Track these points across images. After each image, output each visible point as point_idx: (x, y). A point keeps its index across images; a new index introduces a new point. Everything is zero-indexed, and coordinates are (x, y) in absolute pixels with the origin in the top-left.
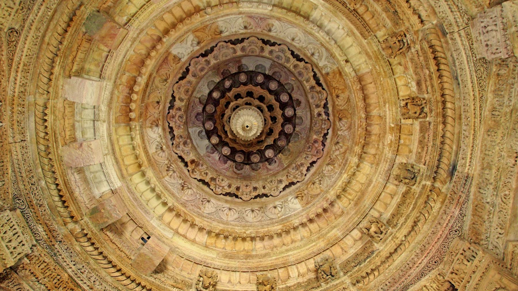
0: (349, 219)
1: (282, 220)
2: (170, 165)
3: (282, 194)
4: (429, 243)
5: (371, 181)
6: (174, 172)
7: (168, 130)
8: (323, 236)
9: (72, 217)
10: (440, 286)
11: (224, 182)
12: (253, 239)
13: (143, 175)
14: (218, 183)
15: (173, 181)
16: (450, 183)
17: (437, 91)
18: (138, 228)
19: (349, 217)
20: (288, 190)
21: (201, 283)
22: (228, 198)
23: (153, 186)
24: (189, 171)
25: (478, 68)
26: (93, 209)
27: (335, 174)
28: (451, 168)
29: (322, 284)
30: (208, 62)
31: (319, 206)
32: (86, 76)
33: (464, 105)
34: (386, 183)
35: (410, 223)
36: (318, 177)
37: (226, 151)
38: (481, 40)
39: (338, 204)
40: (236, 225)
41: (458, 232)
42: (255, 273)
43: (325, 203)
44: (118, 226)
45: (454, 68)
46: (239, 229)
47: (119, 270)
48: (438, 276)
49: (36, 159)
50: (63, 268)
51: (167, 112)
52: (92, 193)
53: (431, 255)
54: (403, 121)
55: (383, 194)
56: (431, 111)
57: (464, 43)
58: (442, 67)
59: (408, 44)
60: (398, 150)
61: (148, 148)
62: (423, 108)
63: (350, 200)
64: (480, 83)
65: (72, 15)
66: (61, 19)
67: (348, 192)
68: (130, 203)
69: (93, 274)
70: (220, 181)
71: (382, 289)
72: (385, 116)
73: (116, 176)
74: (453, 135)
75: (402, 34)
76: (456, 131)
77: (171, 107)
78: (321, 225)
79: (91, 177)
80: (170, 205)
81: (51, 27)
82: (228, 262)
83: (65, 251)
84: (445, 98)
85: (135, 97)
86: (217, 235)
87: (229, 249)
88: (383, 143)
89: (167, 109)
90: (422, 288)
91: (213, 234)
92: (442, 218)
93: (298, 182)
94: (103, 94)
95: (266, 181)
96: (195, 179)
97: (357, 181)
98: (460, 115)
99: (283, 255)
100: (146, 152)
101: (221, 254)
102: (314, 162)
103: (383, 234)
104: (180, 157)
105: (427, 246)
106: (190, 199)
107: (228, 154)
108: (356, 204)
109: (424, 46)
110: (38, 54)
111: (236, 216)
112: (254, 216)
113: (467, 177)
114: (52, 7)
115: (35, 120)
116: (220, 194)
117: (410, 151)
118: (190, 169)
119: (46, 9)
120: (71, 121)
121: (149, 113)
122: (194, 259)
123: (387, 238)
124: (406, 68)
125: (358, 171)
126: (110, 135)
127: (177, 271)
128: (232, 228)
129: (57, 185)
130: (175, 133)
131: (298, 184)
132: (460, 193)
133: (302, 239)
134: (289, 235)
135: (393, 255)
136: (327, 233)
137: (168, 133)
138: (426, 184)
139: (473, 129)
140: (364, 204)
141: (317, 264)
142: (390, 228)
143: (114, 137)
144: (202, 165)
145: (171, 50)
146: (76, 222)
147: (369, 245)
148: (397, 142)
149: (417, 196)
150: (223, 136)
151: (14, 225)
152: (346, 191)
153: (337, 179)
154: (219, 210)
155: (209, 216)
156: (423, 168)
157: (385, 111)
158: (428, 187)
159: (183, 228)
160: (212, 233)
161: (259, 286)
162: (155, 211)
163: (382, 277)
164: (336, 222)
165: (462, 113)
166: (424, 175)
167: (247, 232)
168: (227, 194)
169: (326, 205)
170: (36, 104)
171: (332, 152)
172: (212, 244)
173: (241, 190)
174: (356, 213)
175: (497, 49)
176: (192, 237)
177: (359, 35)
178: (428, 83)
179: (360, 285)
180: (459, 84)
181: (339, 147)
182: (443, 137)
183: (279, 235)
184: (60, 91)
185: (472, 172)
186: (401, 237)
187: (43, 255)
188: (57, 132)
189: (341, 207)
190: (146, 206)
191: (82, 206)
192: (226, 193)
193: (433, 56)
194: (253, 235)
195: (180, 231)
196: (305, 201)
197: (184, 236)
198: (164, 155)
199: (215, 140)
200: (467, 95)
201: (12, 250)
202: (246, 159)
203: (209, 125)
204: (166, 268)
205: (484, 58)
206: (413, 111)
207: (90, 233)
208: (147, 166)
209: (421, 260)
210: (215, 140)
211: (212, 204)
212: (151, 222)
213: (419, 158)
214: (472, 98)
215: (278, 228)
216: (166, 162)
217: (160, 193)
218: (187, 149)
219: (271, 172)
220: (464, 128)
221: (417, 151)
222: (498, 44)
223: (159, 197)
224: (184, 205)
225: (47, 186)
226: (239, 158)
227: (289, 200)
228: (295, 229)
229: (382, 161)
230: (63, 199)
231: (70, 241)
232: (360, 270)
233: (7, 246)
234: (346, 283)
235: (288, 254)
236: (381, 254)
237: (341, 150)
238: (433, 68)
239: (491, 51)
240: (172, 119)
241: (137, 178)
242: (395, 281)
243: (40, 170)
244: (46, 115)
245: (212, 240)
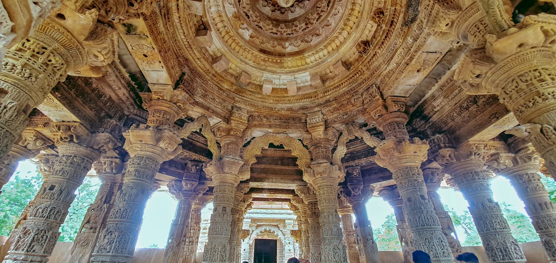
130: (290, 32)
241: (308, 60)
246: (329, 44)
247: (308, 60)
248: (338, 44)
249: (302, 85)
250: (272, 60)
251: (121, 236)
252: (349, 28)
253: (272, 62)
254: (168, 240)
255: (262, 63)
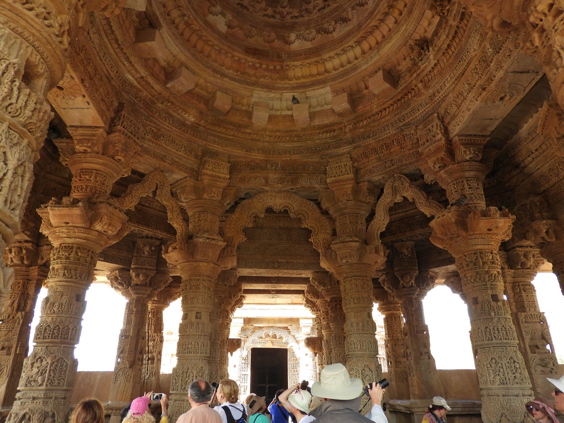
47: (385, 109)
89: (275, 20)
104: (319, 11)
130: (297, 14)
241: (329, 65)
246: (364, 38)
247: (329, 65)
248: (379, 38)
249: (319, 109)
250: (268, 67)
251: (56, 363)
252: (396, 12)
253: (267, 69)
254: (117, 360)
255: (252, 72)
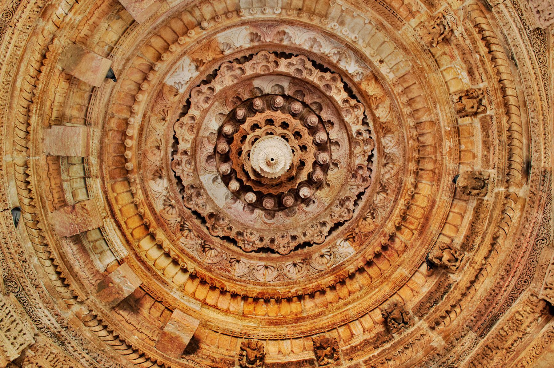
0: (415, 253)
1: (334, 269)
2: (185, 223)
3: (328, 239)
4: (514, 261)
5: (434, 202)
6: (190, 231)
7: (175, 181)
8: (386, 279)
9: (75, 297)
10: (534, 307)
11: (253, 236)
12: (300, 298)
13: (153, 237)
14: (246, 238)
15: (190, 242)
16: (527, 184)
17: (493, 77)
18: (156, 303)
19: (414, 250)
20: (334, 234)
21: (245, 357)
22: (263, 255)
23: (167, 250)
24: (208, 228)
25: (534, 41)
26: (99, 284)
27: (389, 202)
28: (525, 166)
29: (394, 335)
30: (212, 89)
31: (376, 244)
32: (68, 124)
33: (526, 88)
34: (453, 200)
35: (488, 240)
36: (369, 210)
37: (251, 197)
38: (530, 8)
39: (399, 238)
40: (277, 285)
41: (545, 241)
42: (310, 338)
43: (383, 238)
44: (132, 303)
45: (507, 47)
46: (281, 289)
48: (531, 297)
49: (24, 231)
50: (75, 358)
51: (171, 158)
52: (94, 267)
53: (518, 273)
54: (460, 120)
55: (451, 214)
56: (490, 103)
57: (513, 14)
58: (494, 48)
59: (449, 27)
60: (460, 157)
61: (154, 205)
62: (481, 100)
63: (412, 230)
64: (540, 59)
65: (44, 51)
66: (32, 58)
67: (409, 221)
68: (142, 274)
69: (112, 363)
70: (249, 235)
71: (467, 326)
72: (438, 119)
73: (120, 243)
74: (521, 126)
75: (440, 15)
76: (524, 121)
77: (175, 152)
78: (382, 267)
79: (91, 247)
80: (191, 270)
81: (22, 69)
82: (275, 329)
83: (74, 338)
84: (503, 84)
85: (129, 143)
86: (256, 300)
87: (272, 315)
88: (441, 153)
89: (170, 155)
90: (514, 315)
91: (250, 300)
92: (524, 227)
93: (346, 221)
94: (91, 143)
95: (306, 226)
96: (217, 236)
97: (417, 206)
98: (525, 101)
99: (341, 311)
100: (153, 211)
101: (264, 322)
102: (362, 193)
103: (459, 261)
104: (195, 212)
105: (512, 265)
106: (215, 261)
107: (254, 201)
108: (421, 233)
109: (468, 27)
110: (10, 103)
111: (275, 273)
112: (297, 271)
113: (545, 171)
114: (21, 44)
115: (16, 185)
116: (251, 252)
117: (474, 156)
118: (209, 225)
119: (15, 48)
120: (58, 181)
121: (149, 162)
122: (232, 332)
123: (464, 266)
124: (452, 57)
125: (417, 193)
126: (105, 193)
127: (213, 348)
128: (272, 289)
129: (52, 260)
130: (185, 183)
131: (347, 224)
132: (540, 193)
133: (361, 288)
134: (345, 286)
135: (475, 284)
136: (390, 275)
137: (175, 185)
138: (499, 192)
139: (541, 114)
140: (430, 231)
141: (384, 312)
142: (466, 253)
143: (111, 196)
144: (223, 219)
145: (165, 81)
146: (81, 303)
147: (444, 278)
148: (458, 148)
149: (491, 208)
150: (244, 179)
151: (10, 312)
152: (406, 221)
153: (393, 207)
154: (251, 270)
155: (242, 279)
156: (492, 173)
157: (437, 114)
158: (502, 194)
159: (212, 297)
160: (249, 299)
161: (318, 351)
162: (174, 281)
163: (464, 313)
164: (401, 260)
165: (526, 97)
166: (496, 180)
167: (292, 291)
168: (260, 250)
169: (383, 241)
170: (15, 164)
171: (381, 176)
172: (250, 312)
173: (276, 243)
174: (422, 244)
175: (550, 14)
176: (225, 307)
177: (390, 26)
178: (481, 70)
179: (441, 327)
180: (516, 65)
181: (389, 169)
182: (509, 130)
183: (333, 288)
184: (41, 145)
185: (550, 165)
186: (480, 260)
187: (48, 345)
188: (44, 195)
189: (403, 240)
190: (162, 276)
191: (85, 282)
192: (259, 248)
193: (481, 36)
194: (300, 293)
195: (209, 301)
196: (357, 242)
197: (215, 307)
198: (174, 212)
199: (235, 185)
200: (528, 75)
201: (12, 340)
202: (277, 205)
203: (225, 168)
204: (199, 347)
205: (538, 29)
206: (470, 106)
207: (99, 314)
208: (156, 227)
209: (508, 282)
210: (235, 185)
211: (244, 264)
212: (172, 294)
213: (486, 161)
214: (534, 77)
215: (329, 279)
216: (179, 219)
217: (177, 257)
218: (202, 201)
219: (311, 215)
220: (531, 114)
221: (482, 155)
222: (550, 8)
223: (175, 262)
224: (208, 269)
225: (41, 263)
226: (269, 203)
227: (338, 244)
228: (352, 277)
229: (443, 174)
230: (62, 276)
231: (77, 326)
232: (438, 310)
233: (6, 336)
234: (423, 328)
235: (346, 308)
236: (460, 285)
237: (392, 171)
238: (483, 50)
239: (543, 18)
240: (177, 167)
241: (146, 244)
242: (482, 313)
243: (30, 244)
244: (28, 175)
245: (250, 308)
246: (203, 282)
